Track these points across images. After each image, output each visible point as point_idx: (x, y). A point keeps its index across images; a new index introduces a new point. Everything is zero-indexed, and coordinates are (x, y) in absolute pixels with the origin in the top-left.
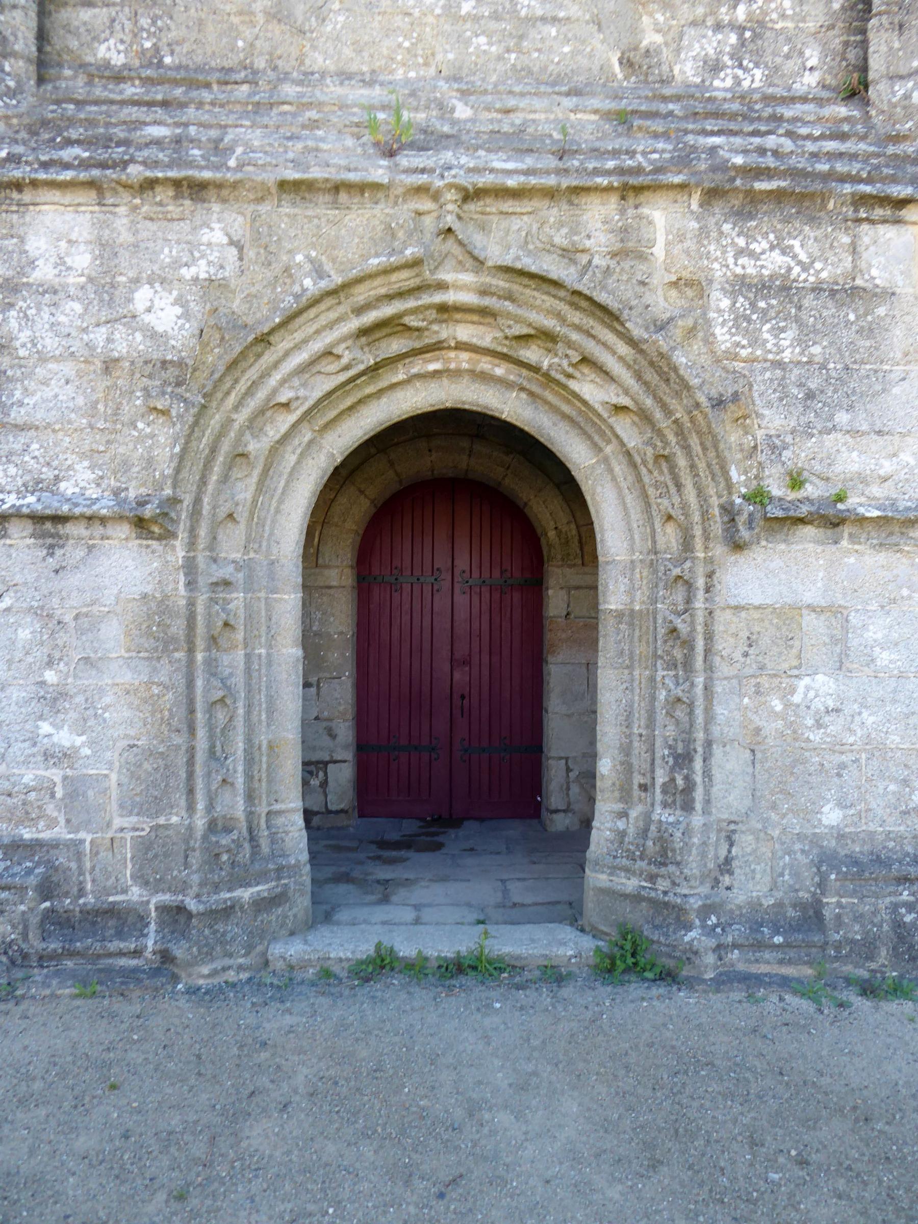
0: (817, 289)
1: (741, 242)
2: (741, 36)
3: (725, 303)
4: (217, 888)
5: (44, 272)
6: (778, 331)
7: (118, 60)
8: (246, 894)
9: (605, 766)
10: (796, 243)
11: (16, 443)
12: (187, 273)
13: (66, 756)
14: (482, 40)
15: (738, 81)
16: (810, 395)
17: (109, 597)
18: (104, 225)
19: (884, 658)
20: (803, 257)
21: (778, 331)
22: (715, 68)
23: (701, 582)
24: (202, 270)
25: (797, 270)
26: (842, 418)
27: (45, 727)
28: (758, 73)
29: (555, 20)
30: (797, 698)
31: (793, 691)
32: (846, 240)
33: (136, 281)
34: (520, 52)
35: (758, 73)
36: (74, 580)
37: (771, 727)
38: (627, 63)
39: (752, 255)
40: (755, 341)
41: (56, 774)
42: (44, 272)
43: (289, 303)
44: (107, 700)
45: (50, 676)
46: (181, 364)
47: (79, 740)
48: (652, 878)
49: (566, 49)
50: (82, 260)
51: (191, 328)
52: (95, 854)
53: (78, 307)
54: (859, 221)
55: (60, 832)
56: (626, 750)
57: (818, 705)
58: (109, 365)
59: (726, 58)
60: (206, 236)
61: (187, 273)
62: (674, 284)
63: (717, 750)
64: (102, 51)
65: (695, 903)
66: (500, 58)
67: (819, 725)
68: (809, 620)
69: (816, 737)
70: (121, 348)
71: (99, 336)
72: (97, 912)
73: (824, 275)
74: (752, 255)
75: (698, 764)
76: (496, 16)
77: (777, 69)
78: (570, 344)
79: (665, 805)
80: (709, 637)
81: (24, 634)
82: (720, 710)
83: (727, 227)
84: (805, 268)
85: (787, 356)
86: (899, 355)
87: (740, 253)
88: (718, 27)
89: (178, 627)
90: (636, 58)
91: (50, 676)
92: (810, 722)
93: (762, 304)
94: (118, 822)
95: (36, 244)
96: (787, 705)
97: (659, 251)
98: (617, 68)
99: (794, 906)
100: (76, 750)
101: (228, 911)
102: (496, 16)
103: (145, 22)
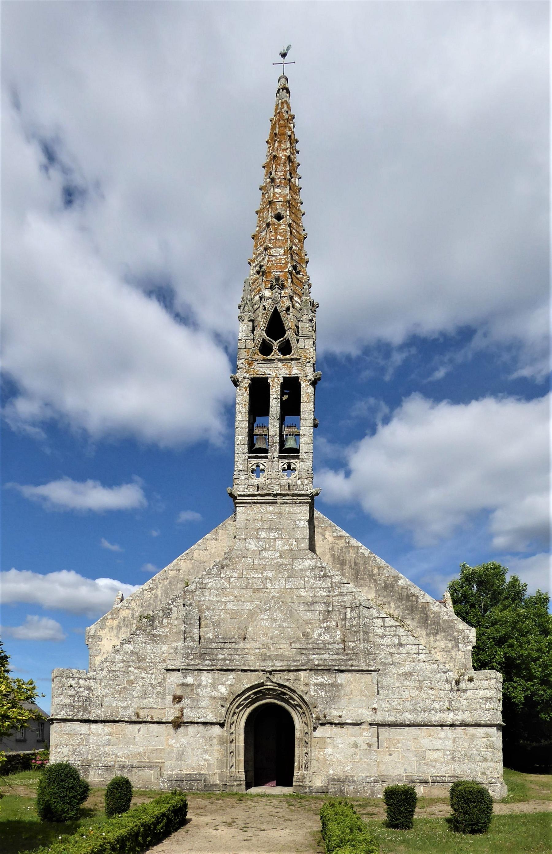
0: (329, 685)
1: (316, 677)
2: (325, 629)
3: (313, 688)
4: (231, 781)
5: (204, 683)
6: (321, 692)
7: (211, 637)
8: (236, 783)
9: (296, 764)
10: (325, 677)
11: (200, 710)
12: (227, 683)
13: (208, 760)
14: (277, 631)
15: (324, 638)
16: (327, 702)
17: (214, 736)
18: (213, 675)
19: (340, 746)
20: (326, 679)
21: (321, 692)
22: (320, 635)
23: (309, 733)
24: (229, 683)
25: (325, 681)
26: (333, 706)
27: (204, 755)
28: (328, 636)
29: (290, 628)
30: (325, 752)
31: (325, 751)
32: (334, 676)
33: (219, 685)
34: (283, 633)
35: (328, 636)
36: (209, 732)
37: (321, 757)
38: (304, 635)
39: (317, 679)
40: (318, 694)
41: (206, 763)
42: (204, 683)
43: (243, 689)
44: (214, 751)
45: (205, 747)
46: (226, 698)
47: (210, 758)
48: (302, 782)
49: (292, 633)
50: (210, 681)
51: (227, 692)
52: (212, 776)
53: (210, 689)
54: (336, 673)
55: (206, 772)
56: (299, 762)
57: (329, 753)
58: (215, 698)
59: (322, 634)
60: (230, 677)
61: (227, 683)
62: (305, 685)
63: (312, 761)
64: (208, 635)
65: (308, 785)
66: (280, 635)
67: (329, 757)
68: (328, 739)
69: (329, 759)
70: (216, 695)
71: (213, 693)
72: (212, 785)
73: (330, 682)
74: (317, 679)
75: (309, 763)
76: (279, 627)
77: (332, 635)
78: (288, 694)
79: (305, 771)
80: (311, 742)
81: (201, 741)
82: (313, 755)
83: (313, 675)
84: (327, 681)
85: (323, 696)
86: (343, 695)
87: (315, 679)
88: (320, 628)
89: (225, 740)
90: (305, 634)
91: (205, 747)
92: (327, 756)
93: (319, 687)
94: (216, 771)
95: (203, 678)
96: (324, 753)
97: (302, 679)
98: (302, 636)
99: (325, 786)
100: (209, 759)
101: (233, 785)
102: (279, 627)
103: (216, 630)
